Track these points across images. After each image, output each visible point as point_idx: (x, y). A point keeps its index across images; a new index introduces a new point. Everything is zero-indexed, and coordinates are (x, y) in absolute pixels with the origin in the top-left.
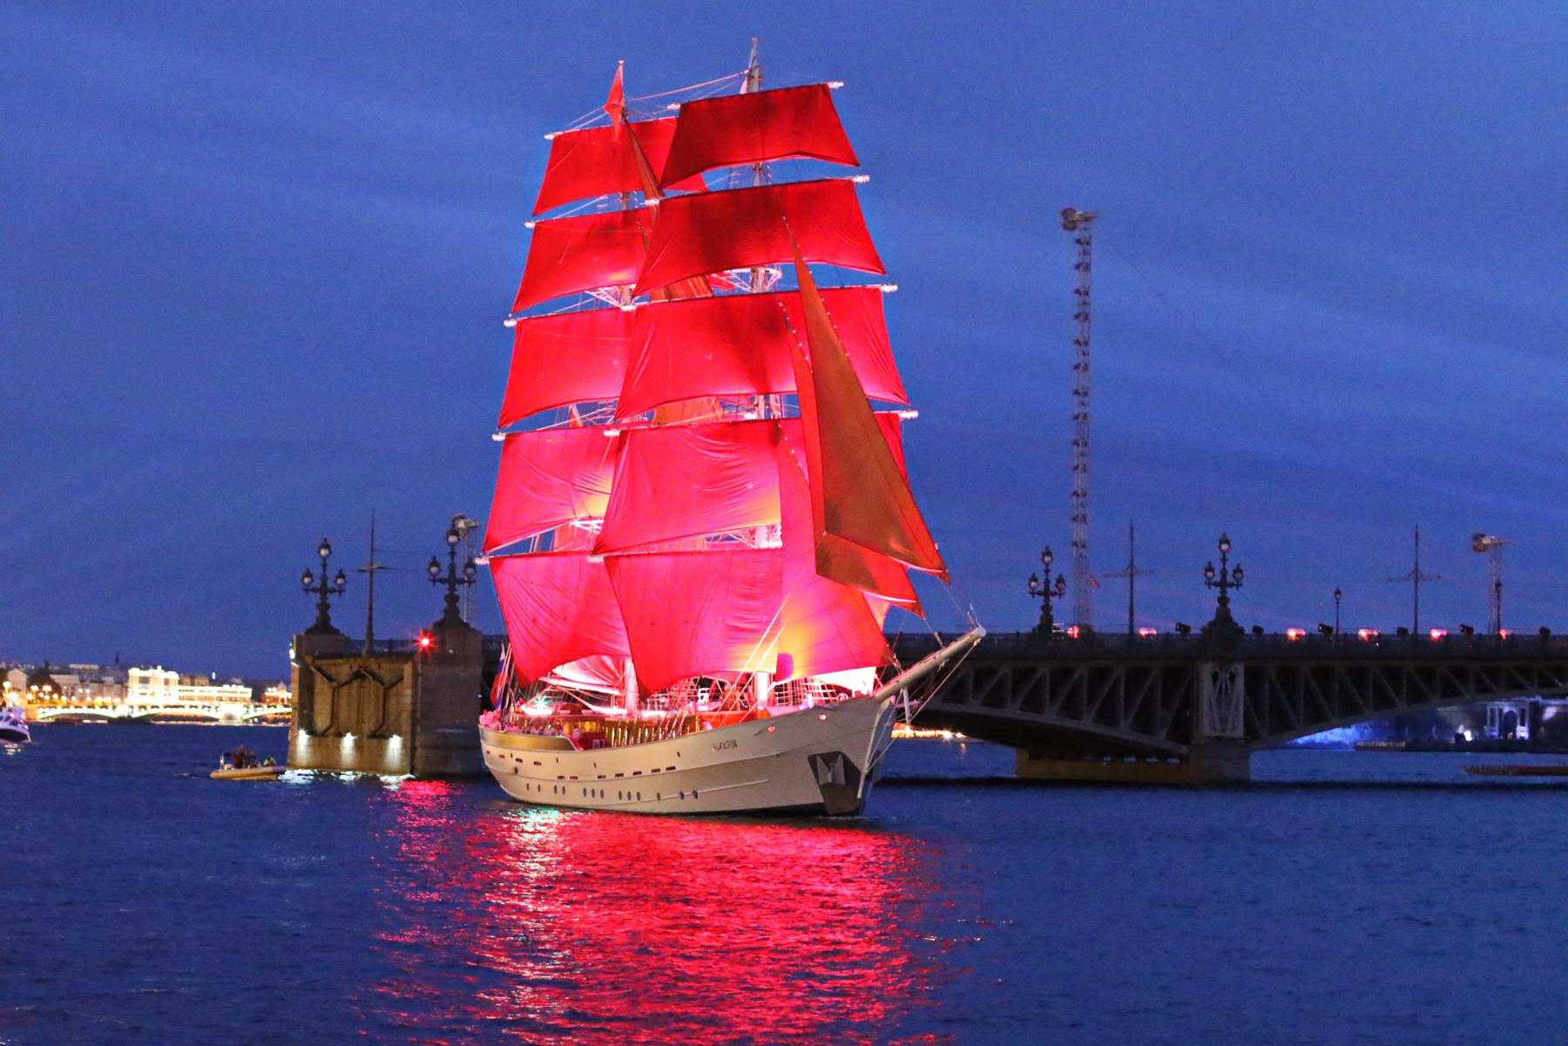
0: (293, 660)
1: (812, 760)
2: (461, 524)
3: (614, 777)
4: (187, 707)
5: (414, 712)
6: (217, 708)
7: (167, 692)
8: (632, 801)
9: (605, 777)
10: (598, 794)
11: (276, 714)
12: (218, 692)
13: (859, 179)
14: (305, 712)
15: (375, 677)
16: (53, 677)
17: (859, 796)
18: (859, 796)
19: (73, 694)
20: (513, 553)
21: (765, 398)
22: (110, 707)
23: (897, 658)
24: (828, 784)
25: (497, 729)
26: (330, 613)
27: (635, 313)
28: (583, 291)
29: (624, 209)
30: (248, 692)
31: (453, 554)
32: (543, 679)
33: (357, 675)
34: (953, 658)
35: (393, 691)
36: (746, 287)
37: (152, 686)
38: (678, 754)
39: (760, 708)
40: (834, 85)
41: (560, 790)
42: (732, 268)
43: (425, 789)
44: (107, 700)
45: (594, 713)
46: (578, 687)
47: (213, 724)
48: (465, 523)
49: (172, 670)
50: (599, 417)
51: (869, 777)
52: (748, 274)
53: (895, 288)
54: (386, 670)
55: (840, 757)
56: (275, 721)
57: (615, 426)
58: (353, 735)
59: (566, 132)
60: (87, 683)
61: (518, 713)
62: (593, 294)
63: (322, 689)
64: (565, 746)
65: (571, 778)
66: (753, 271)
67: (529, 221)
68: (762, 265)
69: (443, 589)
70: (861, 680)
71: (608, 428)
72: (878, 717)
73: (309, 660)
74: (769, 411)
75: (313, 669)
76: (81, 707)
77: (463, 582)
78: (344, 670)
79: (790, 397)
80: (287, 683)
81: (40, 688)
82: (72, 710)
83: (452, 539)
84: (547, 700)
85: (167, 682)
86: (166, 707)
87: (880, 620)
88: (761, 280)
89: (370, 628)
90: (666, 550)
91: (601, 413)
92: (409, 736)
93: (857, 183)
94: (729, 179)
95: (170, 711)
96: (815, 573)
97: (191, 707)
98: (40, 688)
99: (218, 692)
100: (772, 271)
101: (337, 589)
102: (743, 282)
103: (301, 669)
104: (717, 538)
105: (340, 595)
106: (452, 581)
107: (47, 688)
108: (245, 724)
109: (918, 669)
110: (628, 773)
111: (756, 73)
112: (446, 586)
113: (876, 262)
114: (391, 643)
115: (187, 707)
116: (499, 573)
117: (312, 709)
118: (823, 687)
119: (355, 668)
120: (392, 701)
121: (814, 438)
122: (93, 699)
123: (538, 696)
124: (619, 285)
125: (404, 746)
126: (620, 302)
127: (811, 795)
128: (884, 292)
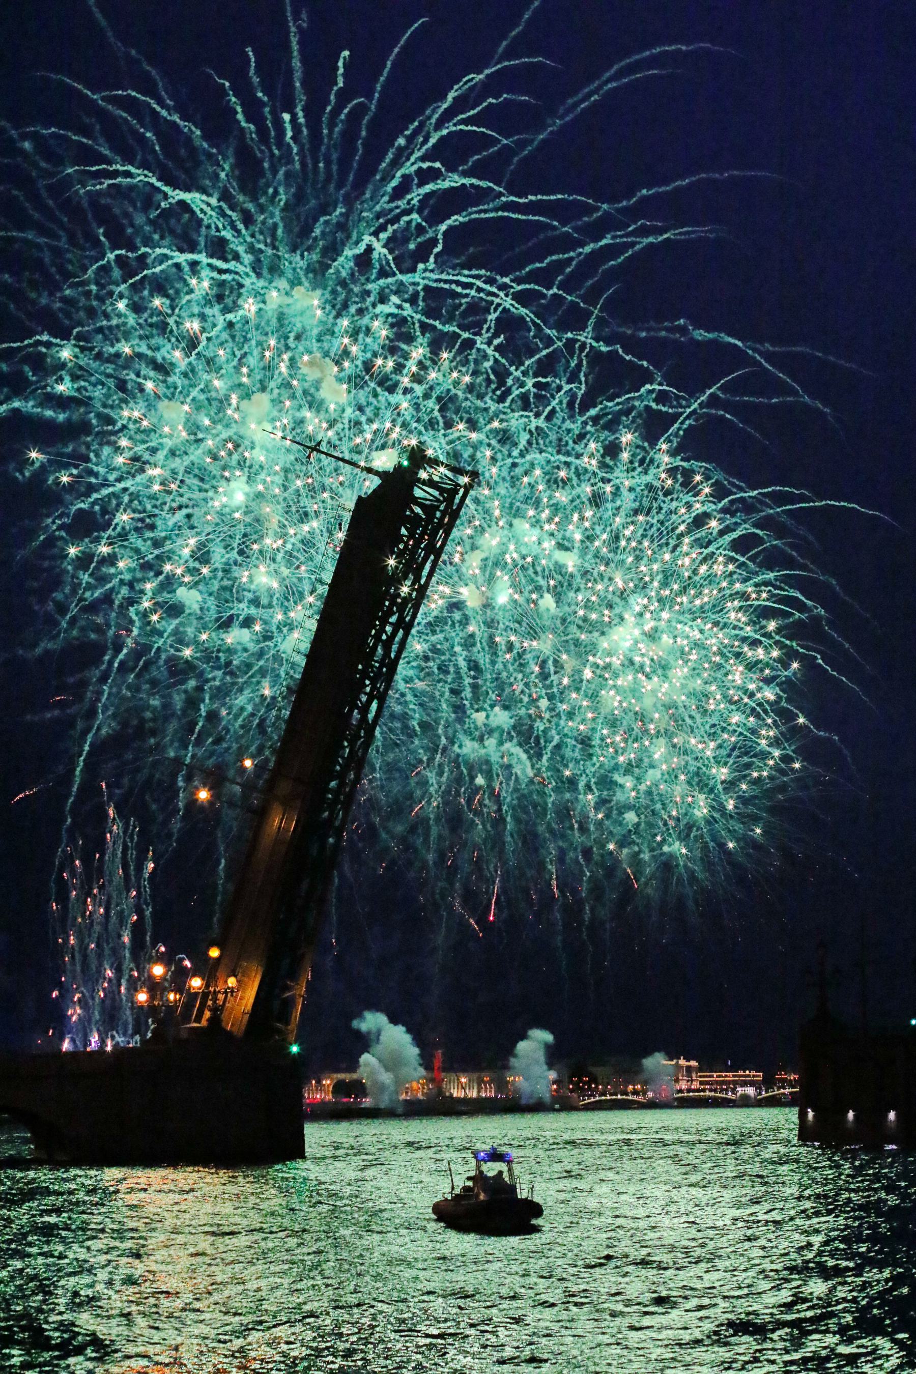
30: (759, 1076)
97: (711, 1090)
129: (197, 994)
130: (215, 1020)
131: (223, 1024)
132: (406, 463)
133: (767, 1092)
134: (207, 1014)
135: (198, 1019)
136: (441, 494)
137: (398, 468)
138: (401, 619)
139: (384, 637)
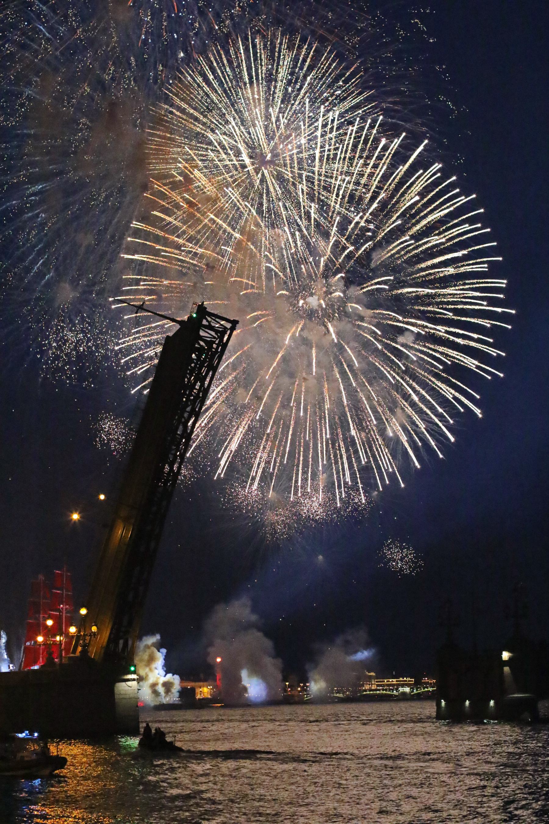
12: (397, 681)
97: (383, 690)
99: (397, 681)
129: (73, 637)
130: (84, 652)
131: (89, 654)
132: (195, 315)
133: (417, 690)
134: (80, 649)
135: (74, 651)
136: (216, 334)
137: (190, 318)
138: (193, 409)
139: (183, 420)
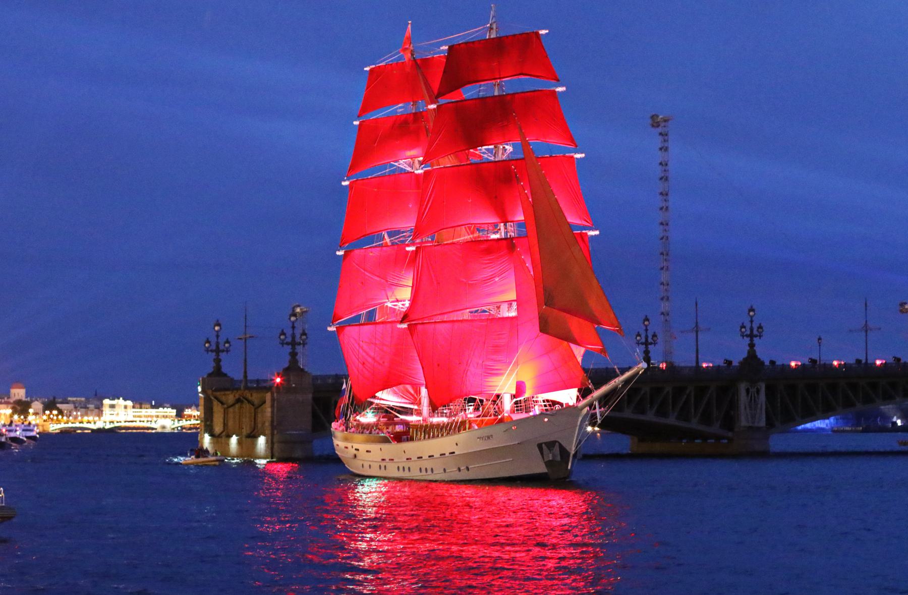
0: (200, 393)
1: (540, 446)
2: (298, 310)
3: (417, 459)
4: (138, 422)
5: (272, 421)
6: (155, 422)
7: (126, 413)
8: (428, 473)
9: (411, 459)
10: (406, 469)
11: (191, 425)
13: (560, 89)
14: (208, 423)
15: (249, 402)
16: (58, 405)
17: (569, 467)
18: (569, 467)
19: (70, 415)
20: (350, 323)
21: (504, 225)
22: (92, 423)
23: (591, 382)
24: (550, 461)
25: (343, 431)
26: (222, 363)
27: (423, 174)
28: (389, 162)
29: (414, 111)
31: (293, 327)
32: (369, 400)
33: (238, 401)
34: (627, 382)
35: (260, 409)
36: (491, 157)
37: (117, 410)
38: (457, 444)
39: (506, 415)
40: (543, 32)
41: (383, 468)
42: (482, 146)
43: (282, 469)
44: (91, 418)
45: (401, 420)
46: (392, 404)
47: (154, 431)
48: (301, 309)
49: (128, 400)
50: (401, 239)
51: (575, 456)
52: (492, 149)
53: (583, 155)
54: (255, 397)
55: (557, 444)
56: (190, 429)
57: (412, 244)
58: (237, 436)
59: (377, 65)
60: (79, 408)
61: (355, 420)
62: (396, 164)
63: (218, 410)
64: (385, 440)
65: (390, 460)
66: (495, 147)
67: (356, 121)
68: (501, 143)
69: (288, 349)
70: (568, 397)
71: (408, 245)
72: (580, 419)
73: (210, 392)
74: (506, 233)
75: (213, 398)
76: (75, 423)
77: (300, 344)
78: (231, 398)
79: (520, 224)
80: (197, 406)
81: (51, 412)
82: (70, 425)
83: (293, 319)
84: (373, 412)
85: (126, 407)
86: (125, 422)
87: (580, 359)
88: (500, 152)
89: (245, 372)
90: (445, 320)
91: (402, 237)
92: (270, 435)
93: (558, 91)
94: (479, 91)
95: (128, 424)
96: (539, 332)
97: (140, 421)
98: (51, 412)
100: (507, 147)
101: (225, 349)
102: (489, 154)
103: (205, 398)
104: (476, 311)
105: (227, 353)
106: (293, 344)
107: (55, 412)
108: (172, 431)
109: (605, 389)
110: (425, 457)
111: (494, 26)
112: (290, 347)
113: (571, 140)
114: (258, 381)
115: (138, 422)
116: (341, 336)
117: (212, 421)
118: (544, 401)
119: (237, 396)
120: (259, 415)
121: (536, 249)
122: (82, 418)
123: (368, 410)
124: (411, 158)
125: (267, 442)
126: (413, 169)
127: (540, 468)
128: (576, 158)
